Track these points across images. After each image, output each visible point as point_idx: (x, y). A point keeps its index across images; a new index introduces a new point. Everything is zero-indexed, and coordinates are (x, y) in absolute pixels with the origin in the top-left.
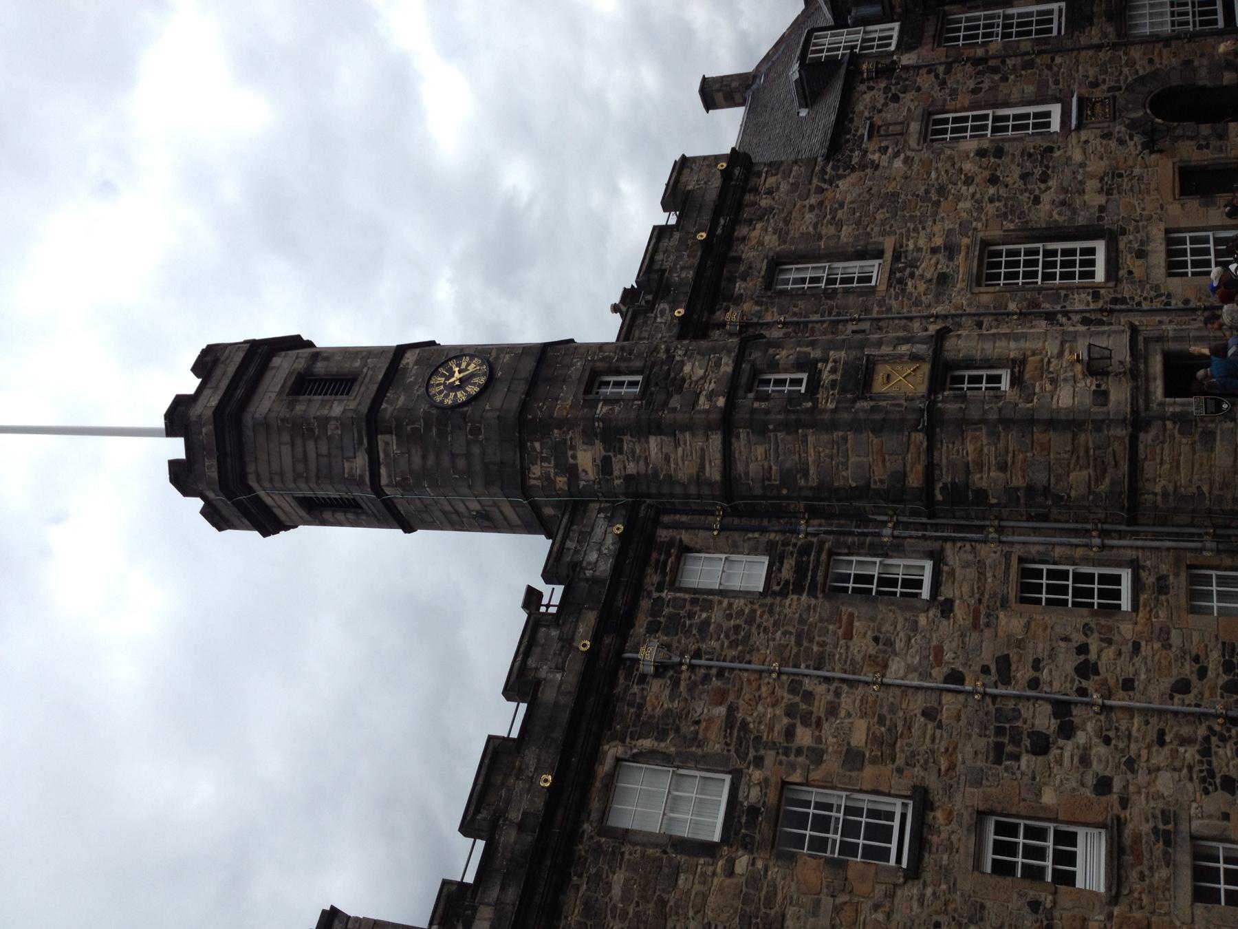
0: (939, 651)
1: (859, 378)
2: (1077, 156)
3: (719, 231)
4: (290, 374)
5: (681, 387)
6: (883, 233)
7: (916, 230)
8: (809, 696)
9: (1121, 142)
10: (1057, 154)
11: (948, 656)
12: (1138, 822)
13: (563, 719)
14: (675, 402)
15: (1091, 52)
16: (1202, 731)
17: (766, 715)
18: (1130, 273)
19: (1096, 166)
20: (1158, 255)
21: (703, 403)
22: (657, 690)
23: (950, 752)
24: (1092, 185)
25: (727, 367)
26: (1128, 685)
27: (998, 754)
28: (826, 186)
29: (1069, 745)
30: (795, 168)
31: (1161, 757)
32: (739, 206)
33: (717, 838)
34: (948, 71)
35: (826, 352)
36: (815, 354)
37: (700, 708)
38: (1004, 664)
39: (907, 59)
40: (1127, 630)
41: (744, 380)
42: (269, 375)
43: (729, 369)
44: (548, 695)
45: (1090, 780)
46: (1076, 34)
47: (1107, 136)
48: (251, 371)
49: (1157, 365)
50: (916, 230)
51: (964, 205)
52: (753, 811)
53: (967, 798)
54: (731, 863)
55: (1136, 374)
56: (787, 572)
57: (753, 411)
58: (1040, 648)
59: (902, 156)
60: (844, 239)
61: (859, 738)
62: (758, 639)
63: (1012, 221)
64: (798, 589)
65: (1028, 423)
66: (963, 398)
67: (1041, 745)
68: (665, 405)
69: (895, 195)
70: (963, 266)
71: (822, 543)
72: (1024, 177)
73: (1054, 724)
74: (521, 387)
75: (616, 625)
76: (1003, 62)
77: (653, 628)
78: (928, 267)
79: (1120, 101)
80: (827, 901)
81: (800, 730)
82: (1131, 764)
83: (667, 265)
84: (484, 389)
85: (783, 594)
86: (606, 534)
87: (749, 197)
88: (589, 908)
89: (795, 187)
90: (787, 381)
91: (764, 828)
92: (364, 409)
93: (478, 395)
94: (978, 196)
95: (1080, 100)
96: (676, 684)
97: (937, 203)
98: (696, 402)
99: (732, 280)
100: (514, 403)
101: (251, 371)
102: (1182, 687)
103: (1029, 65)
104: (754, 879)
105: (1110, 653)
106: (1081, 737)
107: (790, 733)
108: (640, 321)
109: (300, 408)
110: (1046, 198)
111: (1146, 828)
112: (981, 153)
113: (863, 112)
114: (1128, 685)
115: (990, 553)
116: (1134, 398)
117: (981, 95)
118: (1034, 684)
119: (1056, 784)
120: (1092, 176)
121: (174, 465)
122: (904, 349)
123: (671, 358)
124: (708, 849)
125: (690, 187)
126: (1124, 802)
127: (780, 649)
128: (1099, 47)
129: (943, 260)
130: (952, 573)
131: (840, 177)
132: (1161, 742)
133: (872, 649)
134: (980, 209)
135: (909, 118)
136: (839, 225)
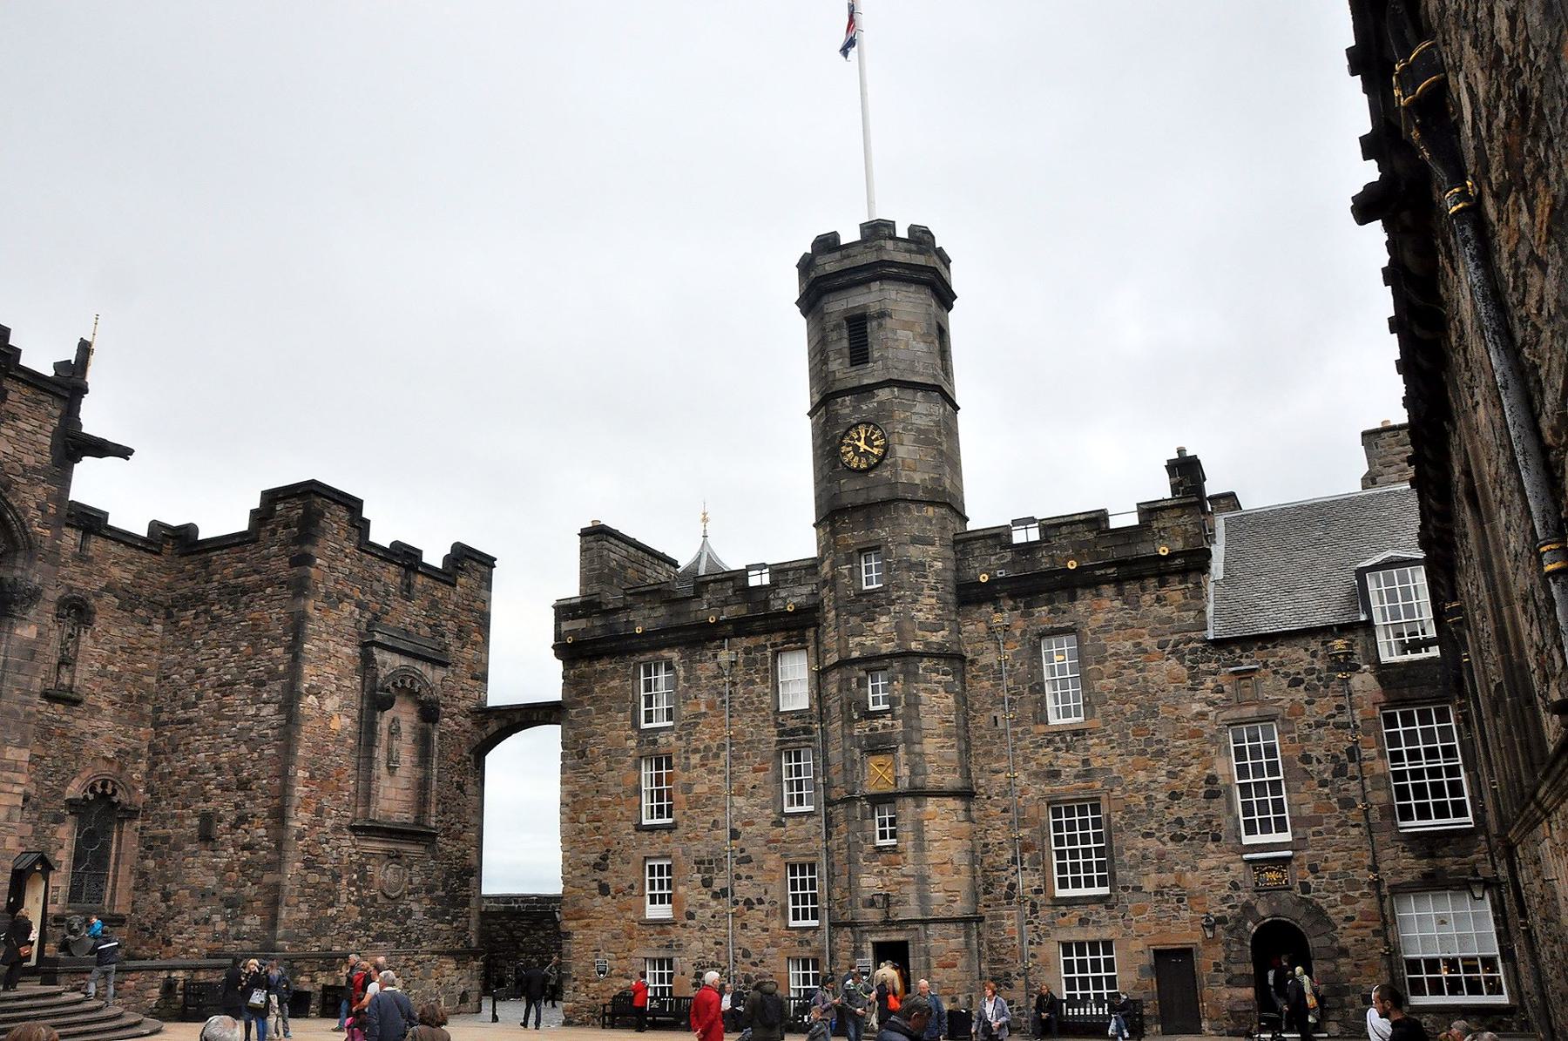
0: (751, 823)
1: (879, 746)
2: (1203, 864)
3: (1098, 573)
4: (866, 306)
5: (864, 620)
6: (1105, 715)
7: (1109, 742)
8: (717, 756)
9: (1224, 900)
10: (1211, 846)
11: (749, 829)
12: (675, 933)
13: (683, 621)
14: (854, 621)
15: (1368, 862)
16: (723, 964)
17: (705, 735)
18: (1064, 915)
19: (1193, 880)
20: (1077, 935)
21: (853, 642)
22: (711, 665)
23: (697, 838)
24: (1168, 878)
25: (886, 648)
26: (744, 926)
27: (699, 862)
28: (1168, 649)
29: (708, 898)
30: (1192, 613)
31: (709, 943)
32: (1140, 578)
33: (644, 726)
34: (1337, 726)
35: (901, 716)
36: (899, 710)
37: (704, 696)
38: (748, 860)
39: (1364, 682)
40: (775, 924)
41: (874, 665)
42: (862, 289)
43: (884, 651)
44: (694, 606)
45: (692, 909)
46: (1401, 845)
47: (1235, 886)
48: (859, 277)
49: (896, 937)
50: (1109, 742)
51: (1142, 777)
52: (655, 742)
53: (676, 848)
54: (631, 738)
55: (887, 923)
56: (791, 724)
57: (849, 680)
58: (758, 879)
59: (1207, 709)
60: (1097, 684)
61: (698, 789)
62: (747, 718)
63: (1122, 818)
64: (781, 734)
65: (851, 861)
66: (864, 818)
67: (707, 883)
68: (851, 614)
69: (1155, 714)
70: (1070, 786)
71: (813, 740)
72: (1179, 822)
73: (717, 889)
74: (859, 501)
75: (740, 627)
76: (1353, 778)
77: (747, 651)
78: (1068, 762)
79: (1285, 894)
80: (620, 789)
81: (698, 756)
82: (703, 928)
83: (1055, 541)
84: (858, 471)
85: (777, 725)
86: (792, 599)
87: (1152, 583)
88: (603, 672)
89: (1170, 620)
90: (876, 695)
91: (648, 750)
92: (838, 386)
93: (854, 470)
94: (1153, 786)
95: (1287, 860)
96: (715, 677)
97: (1143, 753)
98: (854, 635)
99: (1050, 602)
100: (847, 500)
101: (859, 277)
102: (746, 954)
103: (1347, 803)
104: (625, 751)
105: (762, 915)
106: (713, 903)
107: (696, 751)
108: (990, 542)
109: (834, 336)
110: (1150, 842)
111: (673, 937)
112: (1212, 780)
113: (1275, 655)
114: (744, 926)
115: (819, 844)
116: (868, 924)
117: (1300, 765)
118: (738, 877)
119: (691, 893)
120: (1181, 874)
121: (835, 236)
122: (904, 771)
123: (892, 603)
124: (635, 725)
125: (1155, 524)
126: (684, 926)
127: (742, 733)
128: (1374, 868)
129: (1075, 771)
130: (801, 823)
131: (1181, 660)
132: (716, 943)
133: (748, 786)
134: (1138, 791)
135: (1263, 702)
136: (1117, 675)
